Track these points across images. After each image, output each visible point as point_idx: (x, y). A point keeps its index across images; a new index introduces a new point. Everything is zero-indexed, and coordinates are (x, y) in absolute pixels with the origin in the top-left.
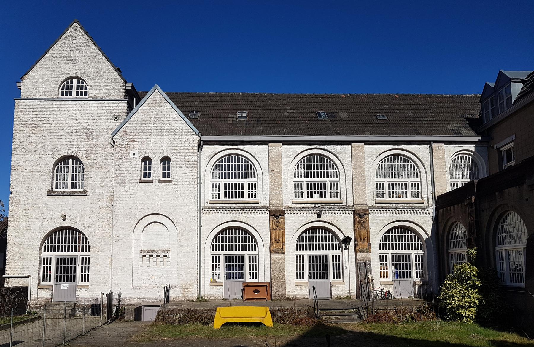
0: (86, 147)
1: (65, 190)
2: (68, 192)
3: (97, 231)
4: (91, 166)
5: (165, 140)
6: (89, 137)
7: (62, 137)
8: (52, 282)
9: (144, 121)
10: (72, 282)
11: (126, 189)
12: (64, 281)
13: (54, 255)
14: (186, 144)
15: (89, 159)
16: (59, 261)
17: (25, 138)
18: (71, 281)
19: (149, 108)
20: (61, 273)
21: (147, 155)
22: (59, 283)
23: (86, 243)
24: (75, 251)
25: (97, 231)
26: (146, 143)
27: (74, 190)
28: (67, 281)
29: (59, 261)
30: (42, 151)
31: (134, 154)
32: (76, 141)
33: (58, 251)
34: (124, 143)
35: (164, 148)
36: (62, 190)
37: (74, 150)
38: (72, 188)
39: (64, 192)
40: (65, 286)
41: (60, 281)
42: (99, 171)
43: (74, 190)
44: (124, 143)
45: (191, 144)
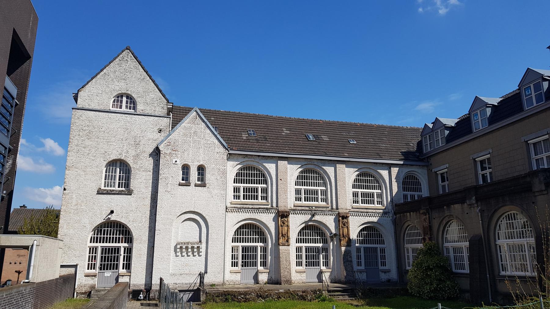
0: (134, 153)
1: (112, 188)
2: (116, 191)
3: (140, 225)
4: (137, 169)
5: (201, 151)
6: (137, 144)
7: (114, 143)
8: (98, 270)
9: (185, 135)
10: (115, 270)
11: (169, 190)
12: (107, 269)
13: (99, 245)
14: (218, 156)
15: (135, 163)
16: (104, 250)
17: (80, 142)
18: (113, 269)
19: (189, 125)
20: (105, 261)
21: (186, 163)
22: (102, 271)
23: (129, 235)
24: (119, 243)
25: (140, 225)
26: (186, 153)
27: (120, 189)
28: (110, 269)
29: (104, 250)
30: (95, 155)
31: (176, 161)
32: (125, 147)
33: (103, 242)
34: (168, 152)
35: (201, 158)
36: (109, 188)
37: (124, 155)
38: (119, 187)
39: (113, 190)
40: (108, 274)
41: (104, 269)
42: (144, 173)
43: (120, 189)
44: (168, 152)
45: (222, 156)
